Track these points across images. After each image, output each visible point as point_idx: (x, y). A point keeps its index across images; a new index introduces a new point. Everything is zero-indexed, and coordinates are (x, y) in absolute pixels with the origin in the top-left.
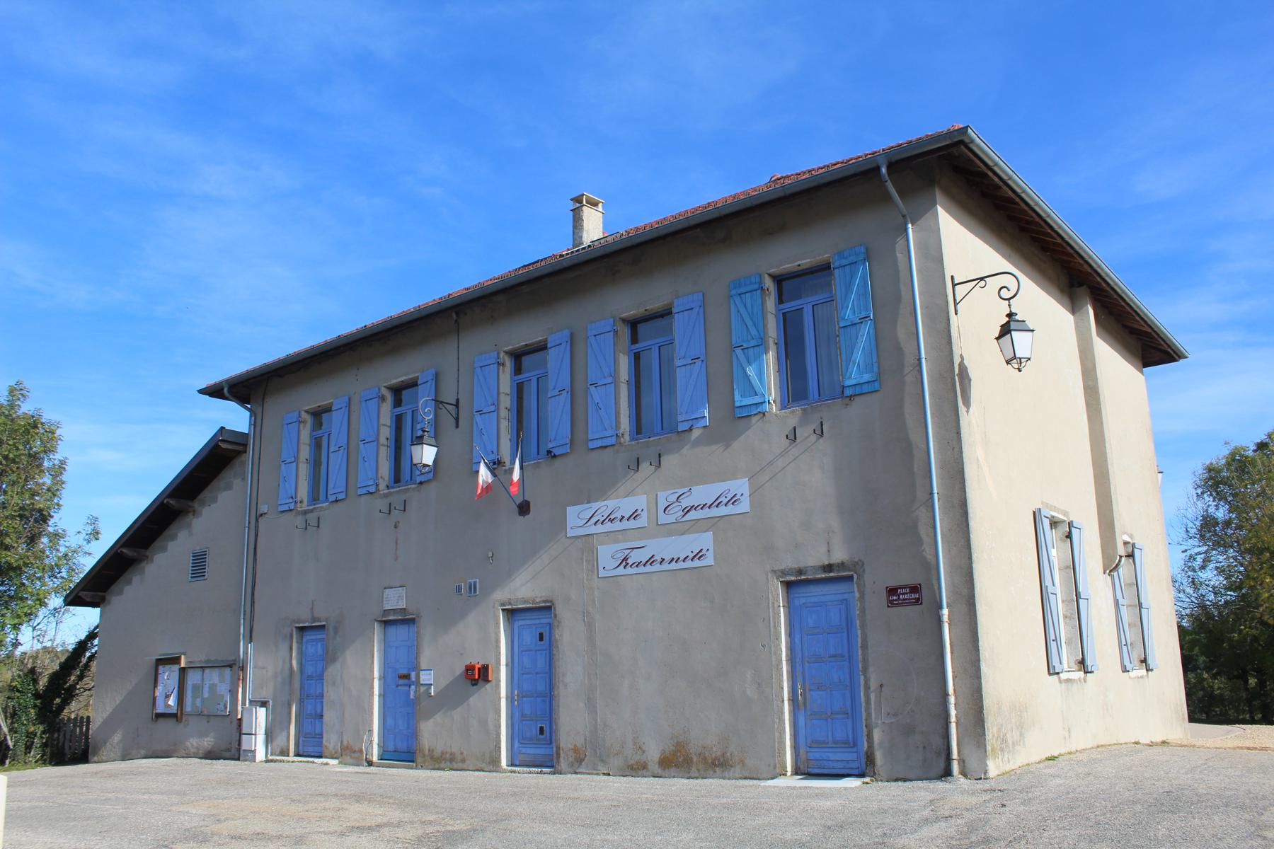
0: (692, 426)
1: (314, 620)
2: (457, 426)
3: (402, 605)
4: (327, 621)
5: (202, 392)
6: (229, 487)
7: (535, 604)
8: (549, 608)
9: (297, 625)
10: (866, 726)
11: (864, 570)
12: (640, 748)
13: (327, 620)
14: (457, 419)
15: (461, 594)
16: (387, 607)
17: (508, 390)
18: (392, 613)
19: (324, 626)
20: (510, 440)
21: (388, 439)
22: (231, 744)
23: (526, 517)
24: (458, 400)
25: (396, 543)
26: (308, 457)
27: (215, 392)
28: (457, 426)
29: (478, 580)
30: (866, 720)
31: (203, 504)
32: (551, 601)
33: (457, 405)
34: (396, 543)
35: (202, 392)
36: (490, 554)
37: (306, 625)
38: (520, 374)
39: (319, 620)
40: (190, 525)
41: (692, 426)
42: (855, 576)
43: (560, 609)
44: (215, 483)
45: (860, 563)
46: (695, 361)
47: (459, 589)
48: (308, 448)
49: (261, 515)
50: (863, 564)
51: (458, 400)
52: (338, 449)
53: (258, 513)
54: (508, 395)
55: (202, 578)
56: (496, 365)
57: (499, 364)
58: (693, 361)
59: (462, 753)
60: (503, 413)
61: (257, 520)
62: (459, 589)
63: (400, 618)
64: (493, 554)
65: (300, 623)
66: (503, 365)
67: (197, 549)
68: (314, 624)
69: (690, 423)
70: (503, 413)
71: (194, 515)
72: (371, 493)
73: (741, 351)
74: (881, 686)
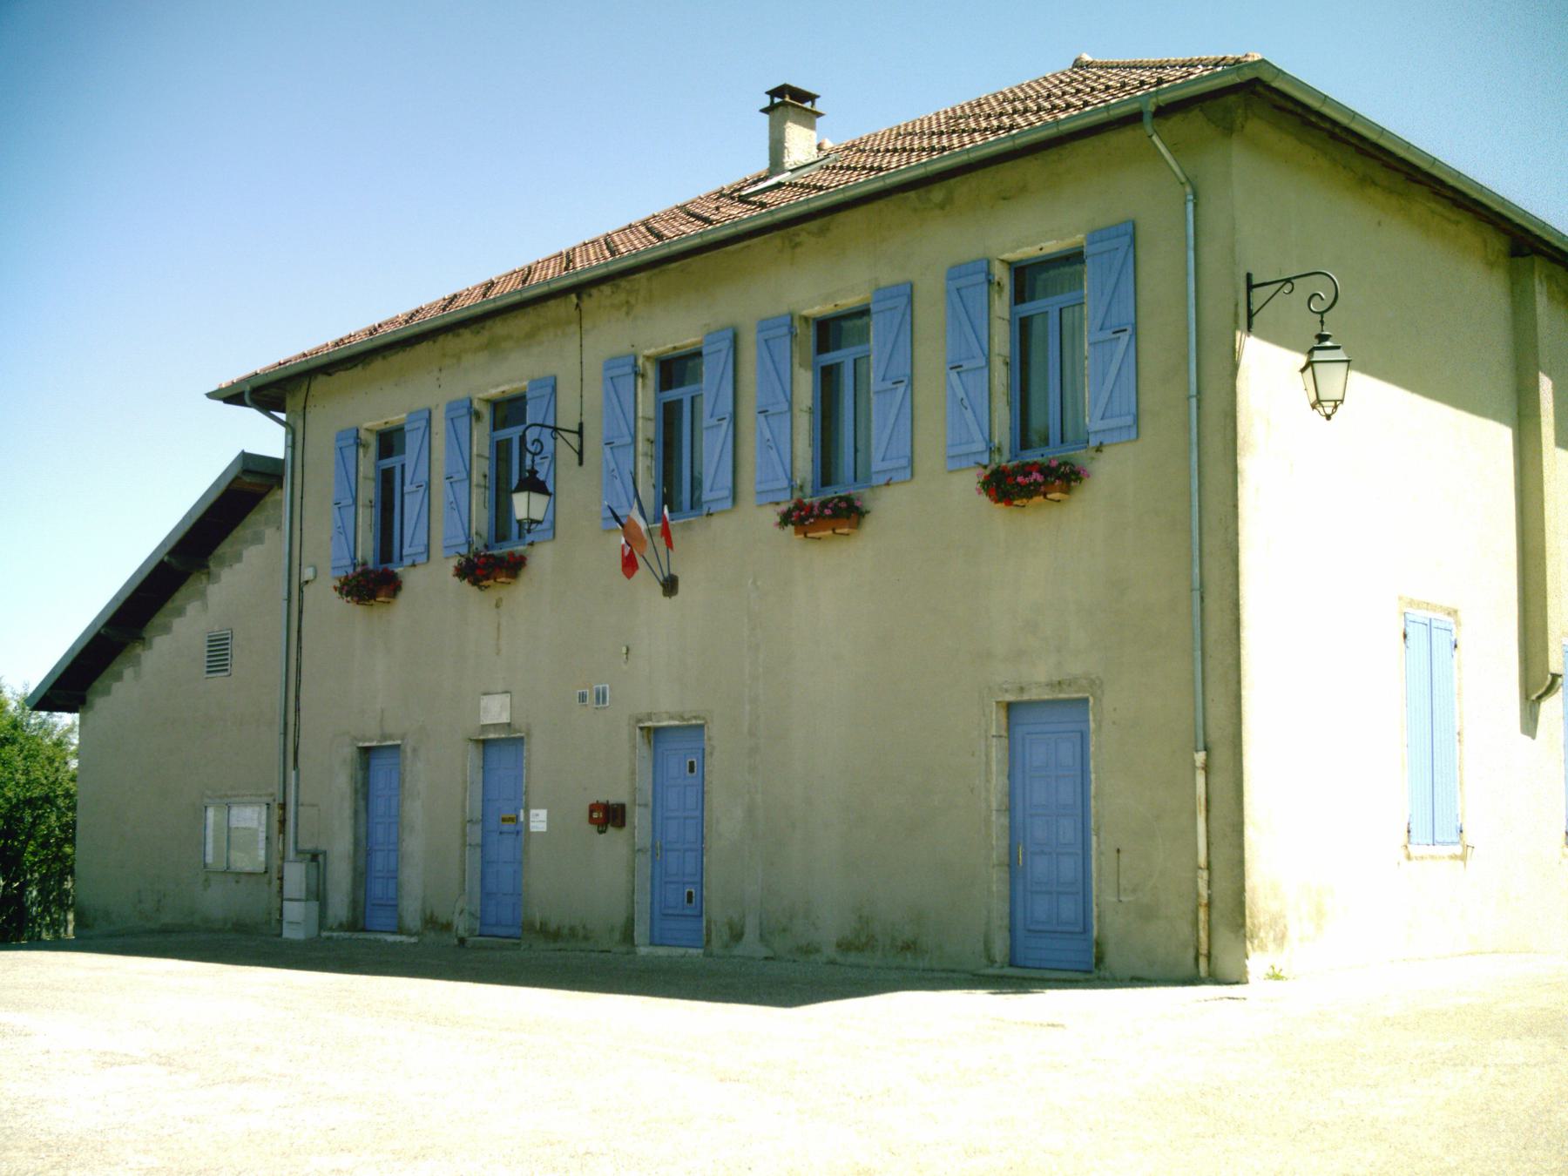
0: (891, 479)
1: (384, 737)
2: (581, 463)
4: (403, 739)
5: (211, 395)
6: (258, 539)
8: (701, 727)
9: (361, 744)
10: (1097, 905)
11: (1103, 691)
14: (580, 454)
15: (586, 705)
17: (651, 413)
19: (398, 746)
20: (654, 486)
21: (485, 476)
22: (270, 914)
23: (673, 598)
24: (581, 425)
25: (498, 628)
26: (372, 497)
27: (232, 396)
28: (581, 463)
29: (608, 686)
30: (1097, 897)
31: (222, 563)
33: (580, 433)
34: (498, 628)
35: (211, 395)
37: (374, 744)
38: (670, 388)
39: (391, 737)
40: (202, 595)
41: (891, 479)
42: (1091, 700)
43: (713, 731)
44: (239, 532)
45: (1097, 682)
47: (583, 698)
48: (372, 484)
49: (307, 582)
50: (1102, 683)
51: (581, 425)
52: (415, 489)
54: (650, 419)
55: (226, 674)
56: (633, 376)
57: (636, 374)
58: (894, 386)
59: (584, 927)
60: (642, 446)
61: (301, 590)
62: (583, 698)
63: (503, 736)
64: (628, 650)
65: (365, 741)
66: (643, 376)
67: (216, 629)
69: (887, 477)
70: (642, 446)
71: (209, 579)
73: (956, 374)
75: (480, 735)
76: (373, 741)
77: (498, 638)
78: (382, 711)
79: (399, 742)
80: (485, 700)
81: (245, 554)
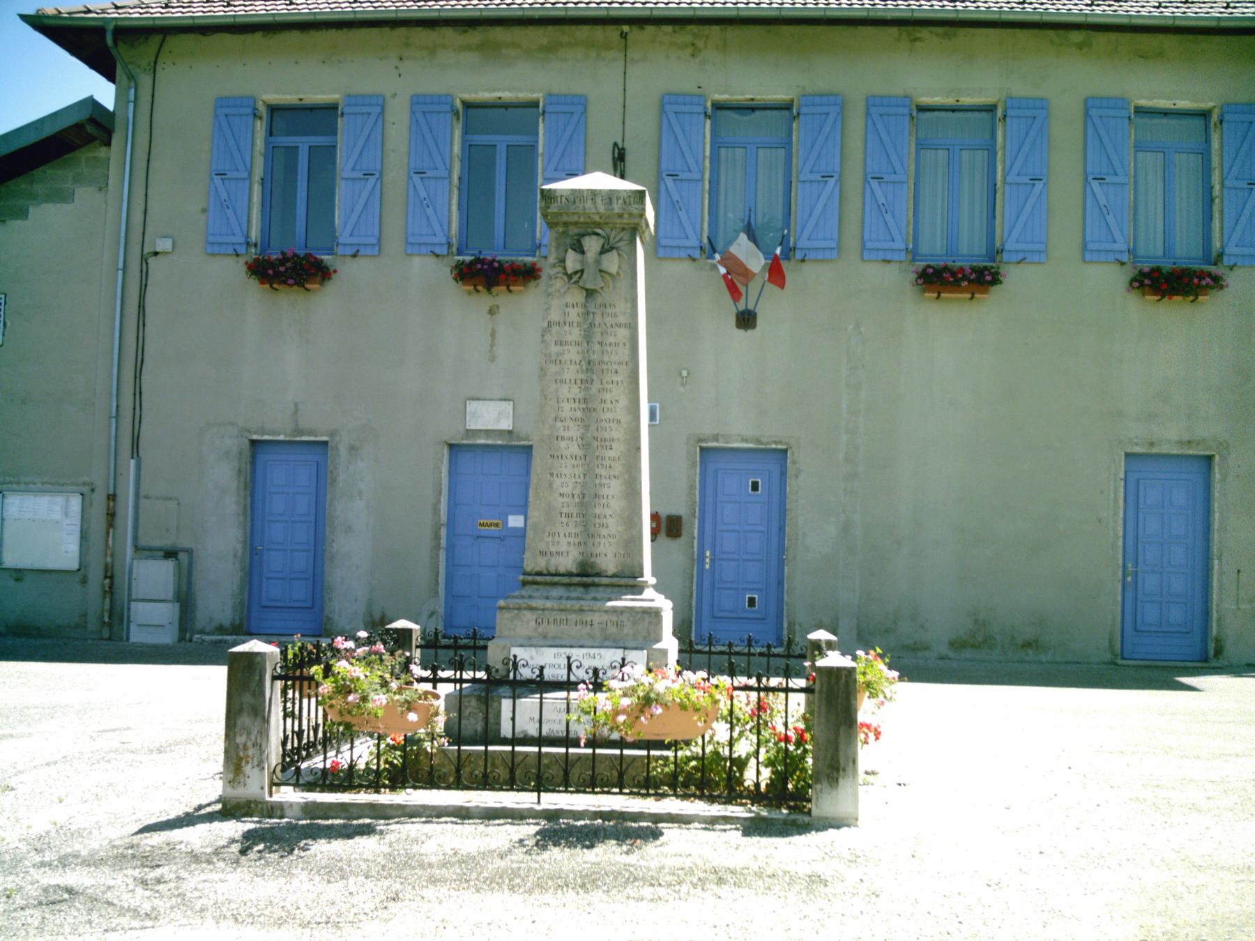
0: (1024, 259)
3: (506, 425)
5: (25, 18)
6: (63, 196)
7: (762, 444)
10: (1217, 612)
12: (922, 626)
13: (332, 434)
16: (472, 425)
18: (483, 434)
19: (326, 443)
22: (85, 616)
29: (658, 405)
32: (786, 444)
35: (25, 18)
36: (685, 373)
37: (281, 438)
45: (1225, 444)
46: (1035, 182)
53: (146, 250)
58: (1032, 182)
63: (499, 442)
64: (688, 374)
65: (263, 434)
68: (298, 439)
72: (437, 256)
74: (1239, 571)
75: (462, 439)
76: (279, 435)
77: (492, 345)
78: (296, 405)
79: (324, 438)
80: (472, 406)
81: (32, 210)
